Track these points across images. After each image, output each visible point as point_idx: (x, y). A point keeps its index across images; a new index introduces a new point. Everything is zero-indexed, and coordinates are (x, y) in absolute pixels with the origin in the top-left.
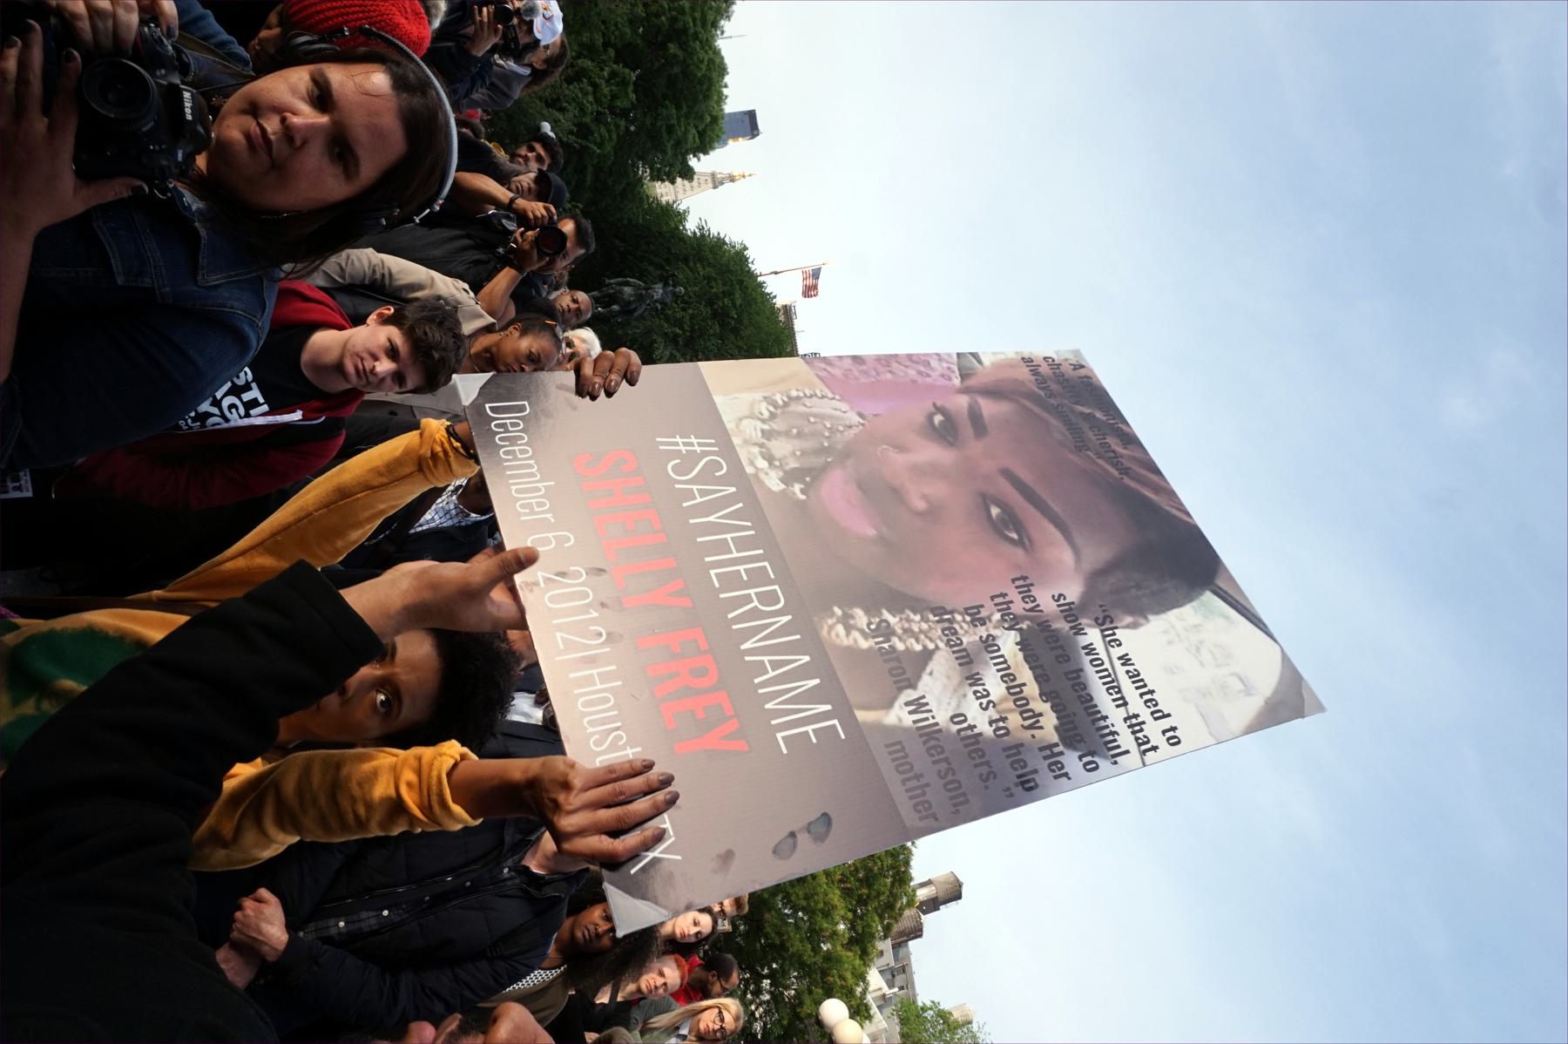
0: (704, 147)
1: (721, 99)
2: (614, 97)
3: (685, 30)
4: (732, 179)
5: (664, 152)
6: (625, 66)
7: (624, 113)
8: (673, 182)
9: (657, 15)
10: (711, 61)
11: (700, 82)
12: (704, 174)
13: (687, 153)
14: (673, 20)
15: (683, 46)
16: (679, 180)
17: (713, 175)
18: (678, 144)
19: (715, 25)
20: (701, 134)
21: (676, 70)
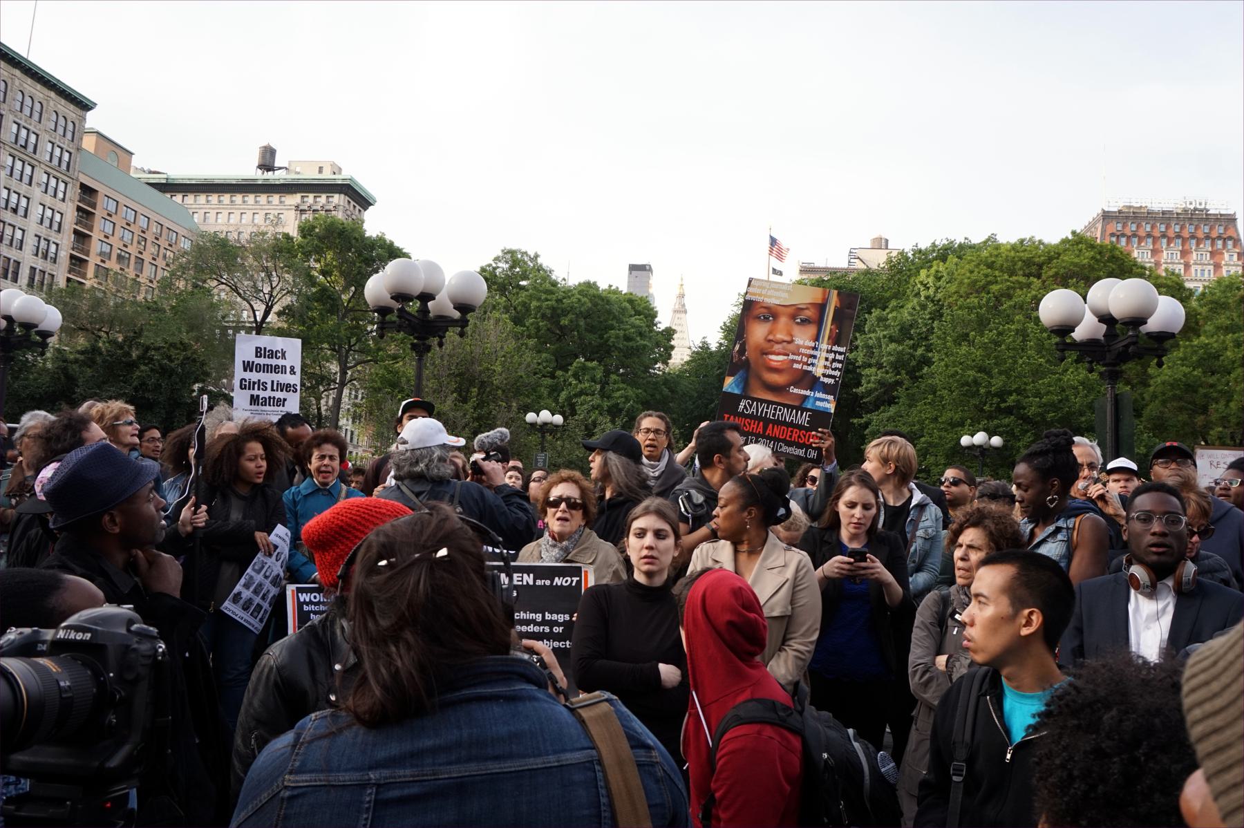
0: (650, 315)
1: (611, 291)
2: (593, 380)
3: (553, 309)
4: (682, 296)
5: (645, 346)
6: (571, 364)
7: (607, 373)
8: (673, 347)
9: (538, 329)
10: (581, 292)
11: (596, 305)
12: (673, 319)
13: (651, 331)
14: (544, 316)
15: (565, 313)
16: (673, 343)
17: (675, 311)
18: (641, 334)
19: (554, 284)
20: (638, 313)
21: (582, 323)
